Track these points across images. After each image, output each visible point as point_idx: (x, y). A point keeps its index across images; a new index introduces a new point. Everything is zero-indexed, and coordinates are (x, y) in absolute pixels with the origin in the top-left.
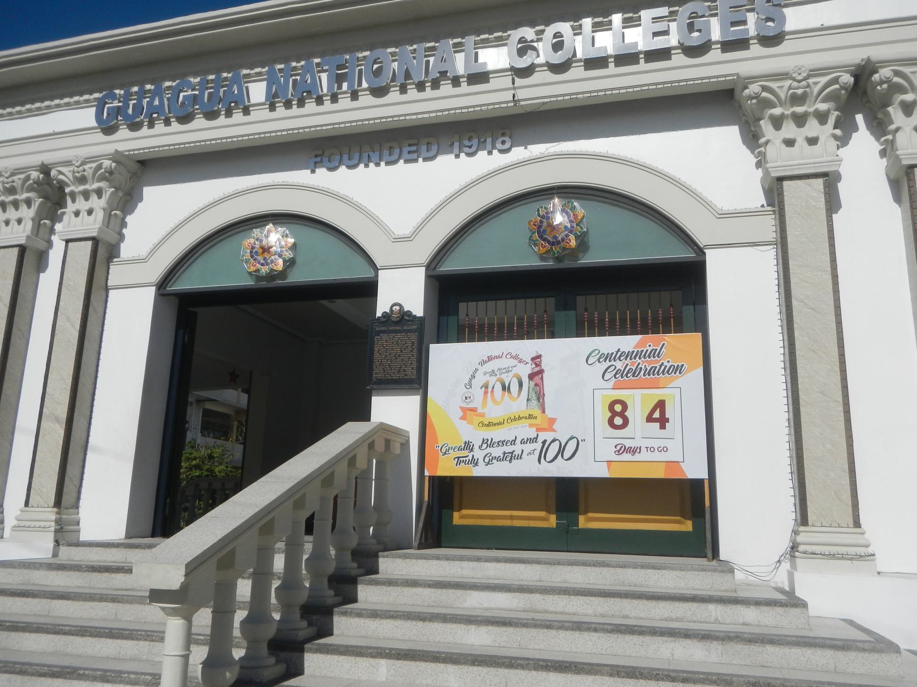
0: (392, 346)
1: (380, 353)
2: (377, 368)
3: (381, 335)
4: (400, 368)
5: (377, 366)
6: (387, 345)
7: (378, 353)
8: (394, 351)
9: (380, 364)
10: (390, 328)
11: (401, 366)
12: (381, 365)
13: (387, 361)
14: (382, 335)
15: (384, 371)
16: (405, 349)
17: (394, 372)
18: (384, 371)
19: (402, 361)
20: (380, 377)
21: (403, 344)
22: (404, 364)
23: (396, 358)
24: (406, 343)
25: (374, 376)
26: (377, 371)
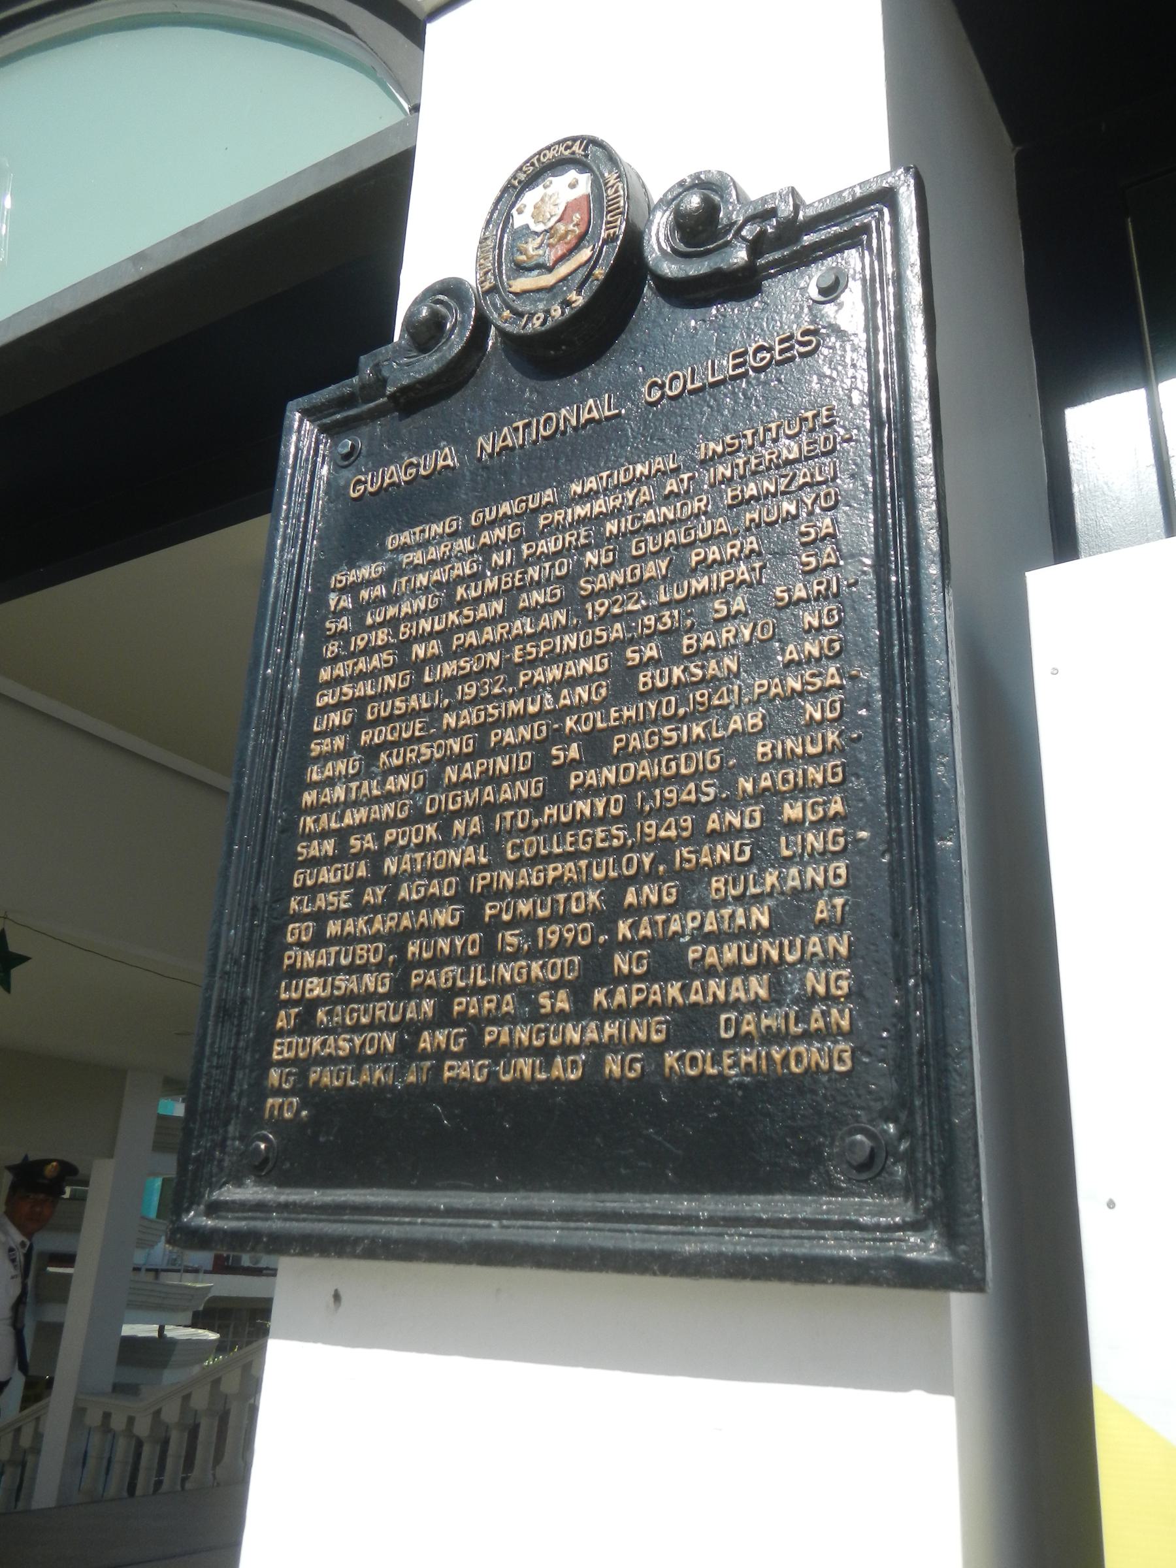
0: (505, 645)
1: (371, 753)
2: (319, 941)
3: (393, 541)
4: (604, 919)
5: (321, 918)
6: (445, 636)
7: (353, 744)
8: (532, 689)
9: (358, 885)
10: (486, 444)
11: (615, 888)
12: (374, 895)
13: (447, 840)
14: (405, 538)
15: (403, 967)
16: (672, 655)
17: (527, 992)
18: (403, 967)
19: (630, 816)
20: (357, 1059)
21: (645, 586)
22: (664, 849)
23: (558, 792)
24: (679, 571)
25: (280, 1050)
26: (315, 988)
